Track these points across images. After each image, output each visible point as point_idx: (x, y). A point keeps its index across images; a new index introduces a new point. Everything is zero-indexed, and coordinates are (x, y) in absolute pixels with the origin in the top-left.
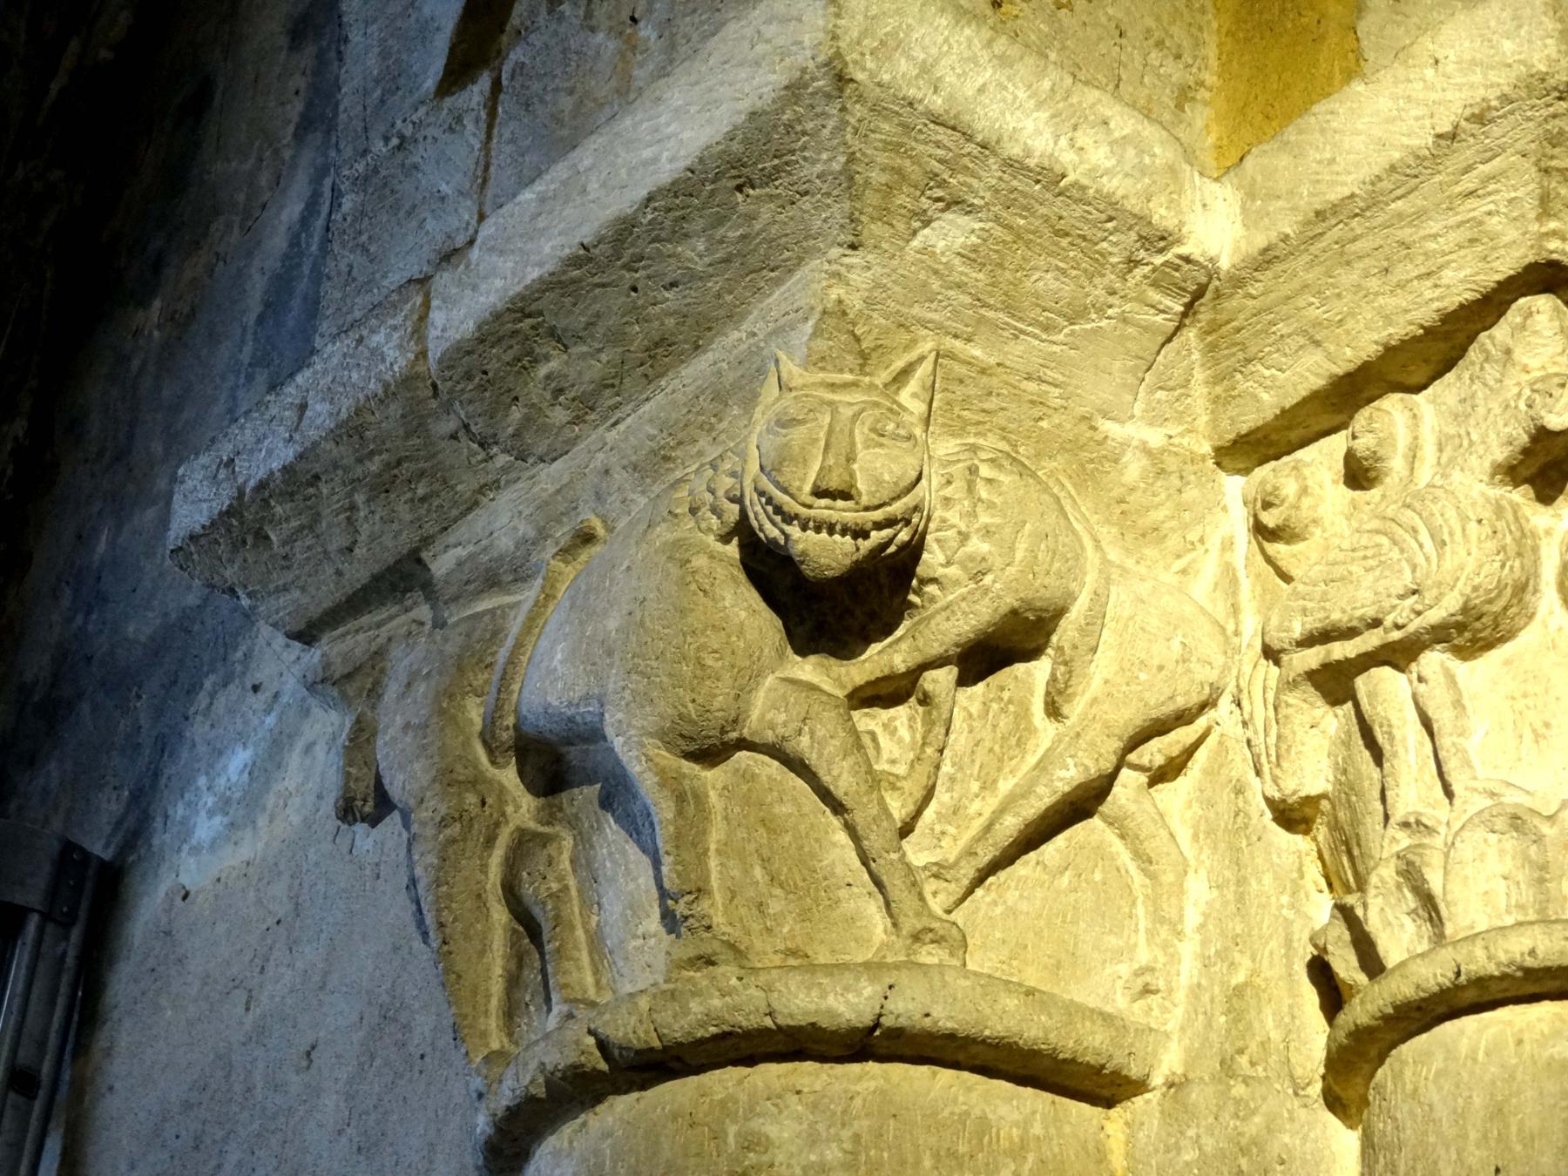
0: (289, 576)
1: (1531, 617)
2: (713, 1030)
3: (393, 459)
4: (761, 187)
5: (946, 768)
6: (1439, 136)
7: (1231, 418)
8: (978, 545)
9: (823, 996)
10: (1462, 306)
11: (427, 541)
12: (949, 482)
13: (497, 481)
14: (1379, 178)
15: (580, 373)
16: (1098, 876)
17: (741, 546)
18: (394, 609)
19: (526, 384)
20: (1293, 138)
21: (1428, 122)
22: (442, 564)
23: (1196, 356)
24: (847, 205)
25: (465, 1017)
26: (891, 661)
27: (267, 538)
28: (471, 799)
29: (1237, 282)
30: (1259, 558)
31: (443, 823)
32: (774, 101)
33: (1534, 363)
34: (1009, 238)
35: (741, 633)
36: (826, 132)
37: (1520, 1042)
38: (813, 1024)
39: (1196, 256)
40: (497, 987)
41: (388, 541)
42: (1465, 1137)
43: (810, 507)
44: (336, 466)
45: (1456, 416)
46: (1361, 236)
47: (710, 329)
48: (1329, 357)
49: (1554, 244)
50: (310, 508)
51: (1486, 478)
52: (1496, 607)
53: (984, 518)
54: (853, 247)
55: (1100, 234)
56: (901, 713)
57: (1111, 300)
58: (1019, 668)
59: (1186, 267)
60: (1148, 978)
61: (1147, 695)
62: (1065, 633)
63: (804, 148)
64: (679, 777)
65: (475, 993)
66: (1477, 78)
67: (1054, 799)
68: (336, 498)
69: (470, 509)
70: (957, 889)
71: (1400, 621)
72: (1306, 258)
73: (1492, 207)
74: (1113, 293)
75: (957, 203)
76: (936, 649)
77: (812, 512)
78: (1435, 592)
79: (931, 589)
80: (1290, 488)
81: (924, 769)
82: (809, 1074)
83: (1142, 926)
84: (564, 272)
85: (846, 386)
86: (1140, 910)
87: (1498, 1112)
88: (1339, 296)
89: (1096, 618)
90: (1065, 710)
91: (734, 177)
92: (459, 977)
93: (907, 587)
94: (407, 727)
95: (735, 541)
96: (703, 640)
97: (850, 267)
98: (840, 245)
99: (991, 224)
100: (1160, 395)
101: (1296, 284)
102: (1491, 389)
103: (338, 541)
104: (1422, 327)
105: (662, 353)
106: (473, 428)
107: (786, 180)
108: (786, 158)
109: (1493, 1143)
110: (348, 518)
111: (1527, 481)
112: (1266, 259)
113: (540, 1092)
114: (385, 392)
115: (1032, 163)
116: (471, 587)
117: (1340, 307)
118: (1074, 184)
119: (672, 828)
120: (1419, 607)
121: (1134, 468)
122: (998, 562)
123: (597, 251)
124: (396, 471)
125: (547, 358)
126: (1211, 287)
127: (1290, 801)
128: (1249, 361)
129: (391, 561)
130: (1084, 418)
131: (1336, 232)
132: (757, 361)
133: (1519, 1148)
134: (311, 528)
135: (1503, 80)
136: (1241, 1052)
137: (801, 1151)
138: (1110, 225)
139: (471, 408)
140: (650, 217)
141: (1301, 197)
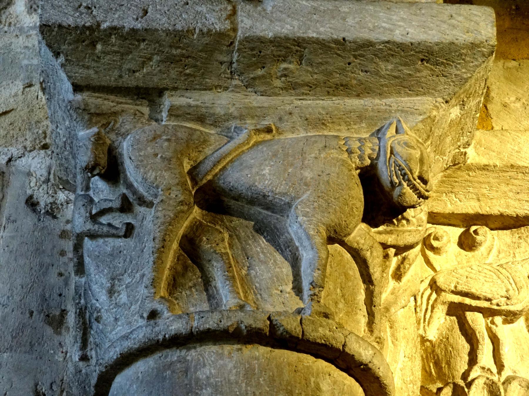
0: (94, 64)
2: (323, 342)
3: (187, 55)
4: (431, 65)
7: (433, 206)
9: (360, 347)
11: (175, 89)
15: (300, 76)
19: (274, 65)
27: (95, 46)
29: (469, 168)
32: (463, 44)
36: (472, 64)
41: (156, 79)
43: (415, 180)
44: (158, 42)
46: (519, 179)
47: (368, 93)
48: (480, 207)
50: (129, 48)
59: (463, 156)
63: (459, 64)
68: (145, 51)
69: (205, 90)
71: (500, 304)
77: (415, 182)
78: (516, 301)
79: (404, 222)
84: (329, 42)
88: (497, 191)
91: (425, 56)
93: (396, 216)
97: (442, 107)
98: (443, 99)
101: (487, 180)
103: (132, 66)
104: (517, 215)
105: (342, 89)
106: (234, 65)
107: (442, 68)
112: (485, 168)
114: (208, 33)
116: (189, 116)
117: (494, 194)
120: (508, 303)
123: (349, 45)
124: (183, 59)
126: (460, 165)
128: (452, 192)
129: (151, 86)
131: (512, 174)
132: (387, 115)
134: (122, 55)
139: (242, 59)
140: (381, 47)
141: (504, 156)
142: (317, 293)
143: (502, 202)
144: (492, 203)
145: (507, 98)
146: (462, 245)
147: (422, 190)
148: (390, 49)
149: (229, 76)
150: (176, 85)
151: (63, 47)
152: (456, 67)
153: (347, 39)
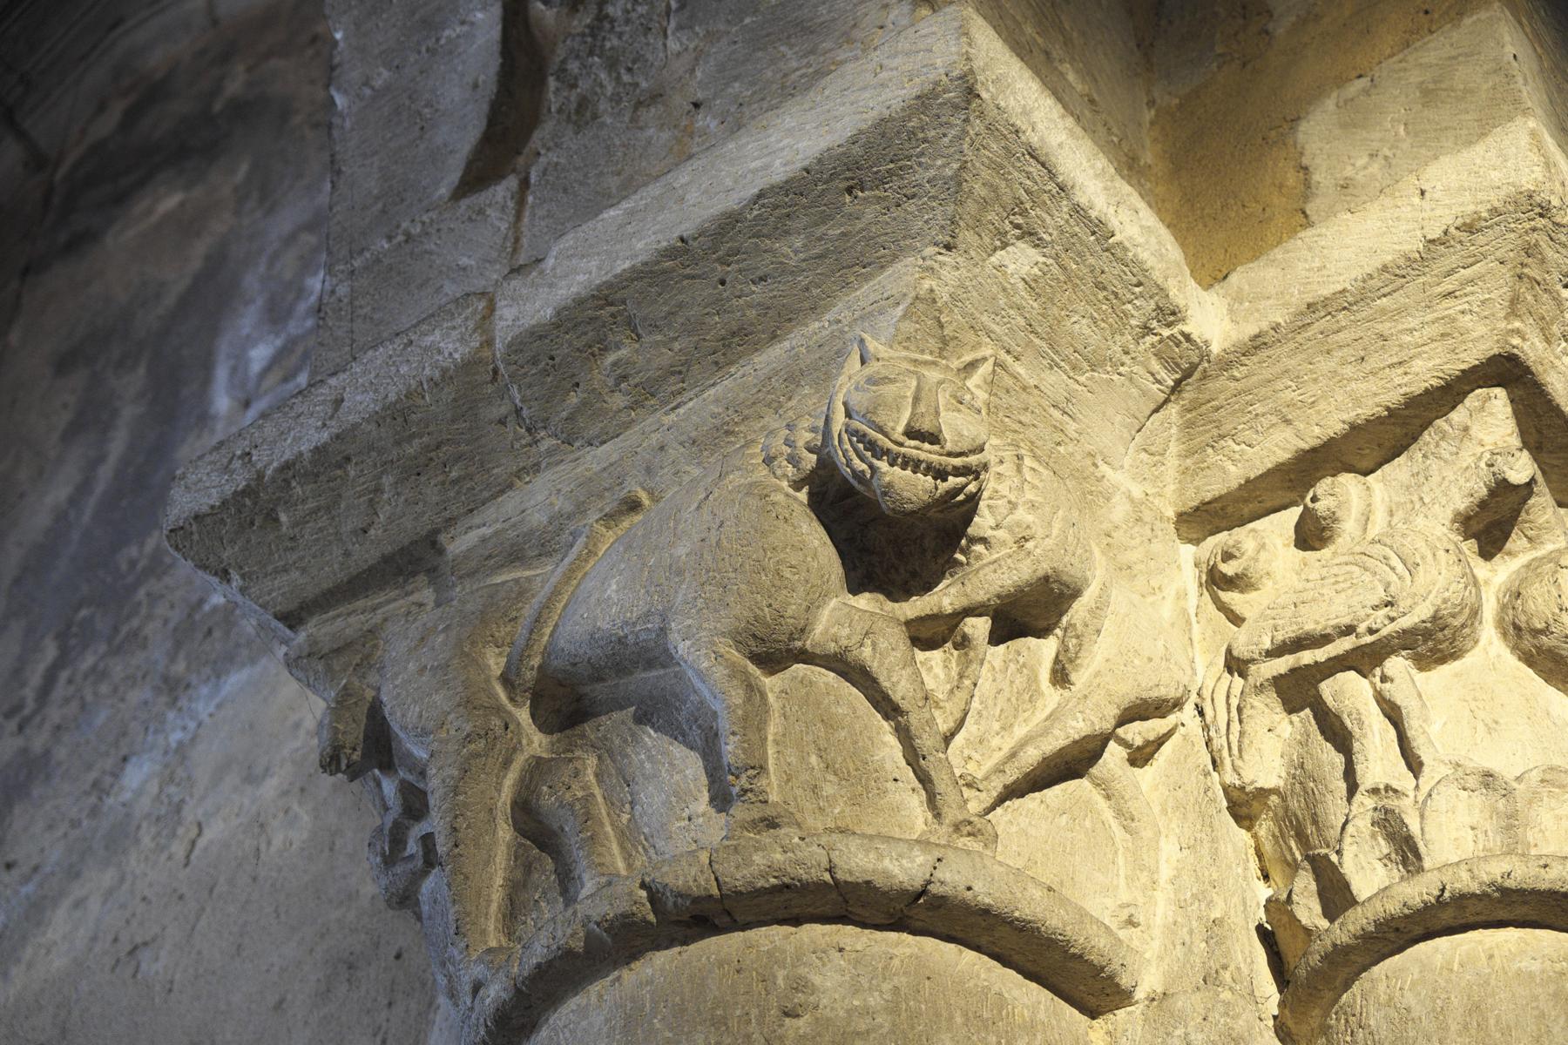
1: (1476, 642)
2: (773, 880)
5: (975, 704)
6: (1432, 241)
7: (1197, 488)
8: (1022, 514)
9: (880, 857)
10: (1427, 391)
11: (451, 521)
12: (1001, 462)
13: (538, 464)
14: (1371, 276)
15: (649, 361)
16: (1088, 823)
17: (810, 494)
18: (393, 594)
19: (591, 370)
20: (1279, 257)
21: (1419, 233)
22: (459, 544)
23: (1174, 430)
24: (951, 208)
25: (468, 914)
26: (940, 602)
27: (277, 520)
28: (496, 722)
29: (1226, 364)
30: (1211, 607)
31: (469, 738)
32: (903, 109)
33: (1488, 440)
34: (1062, 278)
35: (815, 557)
36: (946, 140)
37: (1491, 957)
38: (868, 883)
39: (1194, 336)
40: (497, 896)
42: (1447, 1029)
43: (901, 445)
44: (371, 448)
45: (1408, 488)
47: (790, 320)
49: (1516, 341)
51: (1447, 523)
52: (1457, 623)
53: (1030, 495)
54: (948, 247)
55: (1129, 296)
56: (936, 656)
57: (1126, 359)
58: (1031, 641)
59: (1186, 345)
60: (1132, 910)
61: (1140, 678)
62: (1078, 612)
63: (922, 154)
64: (745, 673)
65: (479, 894)
66: (1468, 196)
67: (1067, 742)
68: (362, 480)
69: (502, 492)
70: (987, 798)
71: (1374, 627)
72: (1292, 345)
73: (1466, 306)
74: (1127, 353)
75: (1031, 234)
76: (981, 596)
77: (903, 450)
78: (1409, 602)
79: (979, 548)
80: (1249, 545)
81: (961, 696)
82: (848, 934)
83: (1122, 873)
84: (657, 263)
85: (926, 363)
86: (1121, 860)
87: (1475, 1008)
88: (1315, 380)
89: (1098, 610)
90: (1073, 677)
91: (847, 179)
92: (467, 878)
94: (422, 670)
95: (805, 490)
96: (782, 556)
97: (942, 264)
99: (1050, 261)
100: (1143, 456)
101: (1278, 369)
102: (1446, 461)
104: (1388, 409)
105: (739, 340)
106: (525, 413)
107: (896, 183)
108: (901, 163)
109: (1473, 1032)
110: (371, 500)
111: (1474, 536)
112: (1257, 344)
113: (578, 945)
114: (443, 376)
115: (1093, 214)
117: (1314, 389)
118: (1119, 244)
119: (740, 712)
121: (1119, 511)
122: (1040, 533)
123: (695, 244)
124: (433, 454)
125: (618, 347)
127: (1248, 789)
128: (1222, 437)
129: (406, 542)
130: (1090, 454)
133: (1498, 1035)
134: (328, 509)
135: (1495, 199)
136: (1225, 967)
137: (844, 998)
138: (1137, 290)
139: (528, 392)
142: (747, 786)
143: (1340, 399)
144: (1318, 412)
145: (1349, 168)
146: (1305, 541)
147: (934, 457)
148: (776, 207)
149: (528, 439)
150: (447, 514)
151: (225, 555)
152: (920, 164)
153: (685, 235)
